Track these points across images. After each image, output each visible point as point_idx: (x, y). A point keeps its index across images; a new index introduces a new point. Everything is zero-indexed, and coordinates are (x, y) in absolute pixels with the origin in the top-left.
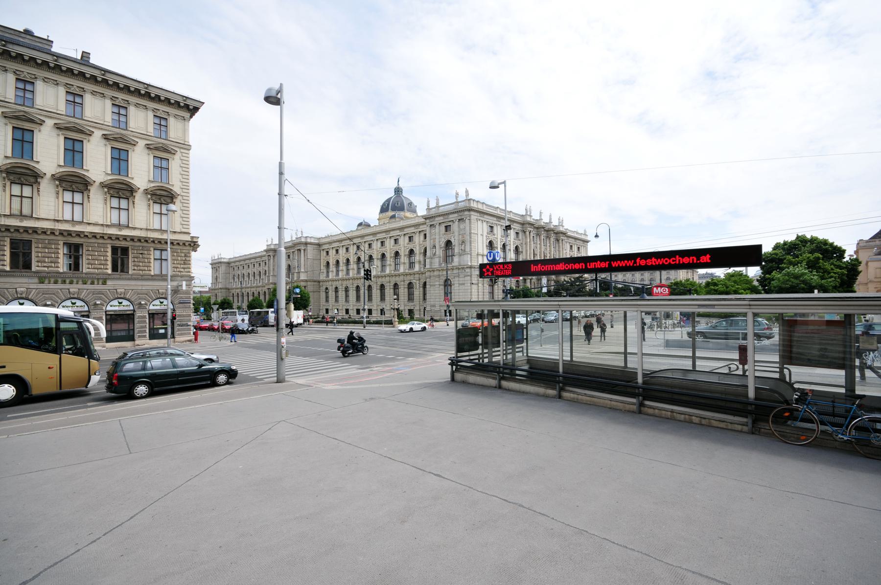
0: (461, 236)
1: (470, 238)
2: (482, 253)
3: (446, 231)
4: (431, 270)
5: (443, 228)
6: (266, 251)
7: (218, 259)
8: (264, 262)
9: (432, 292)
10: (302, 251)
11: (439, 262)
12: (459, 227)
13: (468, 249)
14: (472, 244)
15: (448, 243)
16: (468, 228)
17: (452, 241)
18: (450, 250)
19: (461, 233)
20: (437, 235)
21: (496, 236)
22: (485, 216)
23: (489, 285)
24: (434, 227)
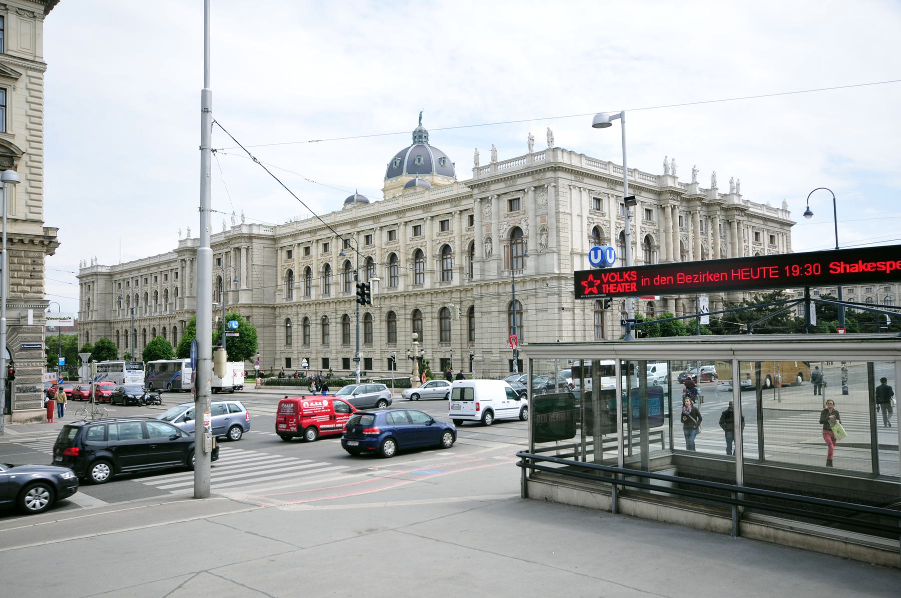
0: (539, 219)
1: (558, 221)
2: (580, 251)
3: (511, 210)
4: (483, 283)
5: (504, 204)
6: (178, 252)
7: (92, 267)
8: (174, 272)
9: (484, 325)
10: (243, 252)
11: (499, 267)
12: (535, 201)
13: (552, 243)
14: (562, 234)
15: (516, 232)
16: (552, 204)
17: (523, 227)
19: (540, 212)
20: (493, 216)
22: (586, 180)
23: (595, 312)
24: (488, 202)
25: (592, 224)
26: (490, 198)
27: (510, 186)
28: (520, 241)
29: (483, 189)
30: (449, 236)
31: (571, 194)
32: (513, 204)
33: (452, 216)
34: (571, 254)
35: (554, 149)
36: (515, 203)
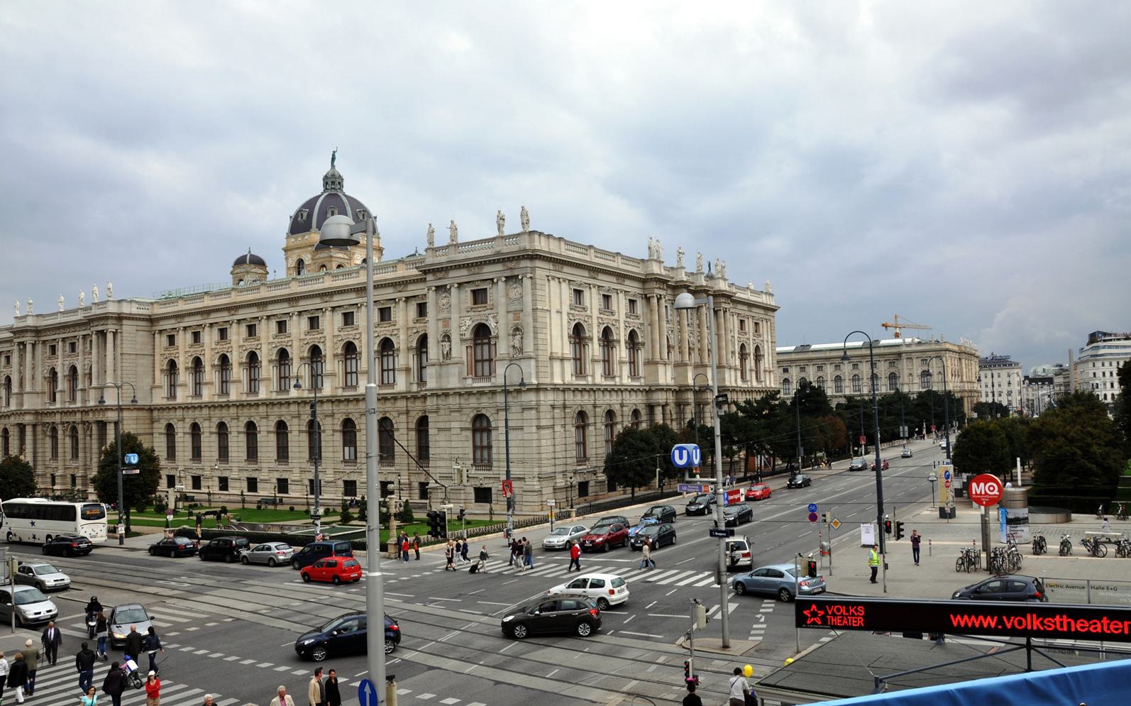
1: (535, 320)
2: (560, 355)
3: (475, 303)
5: (467, 296)
11: (460, 373)
13: (529, 348)
14: (540, 336)
15: (481, 332)
16: (528, 299)
17: (491, 324)
18: (486, 347)
19: (512, 308)
20: (453, 310)
21: (588, 313)
22: (566, 269)
23: (577, 427)
24: (445, 291)
26: (448, 287)
27: (475, 274)
28: (487, 341)
29: (439, 275)
30: (391, 328)
31: (549, 286)
32: (479, 296)
33: (396, 303)
34: (550, 359)
35: (530, 232)
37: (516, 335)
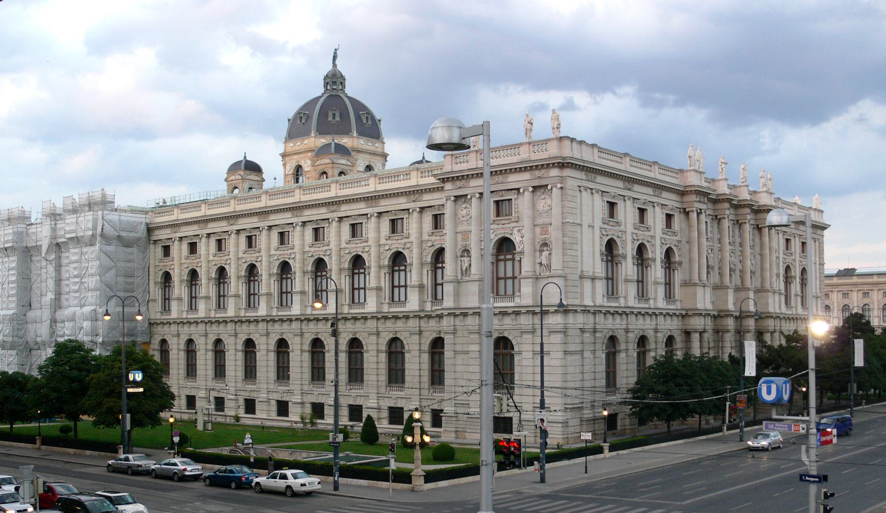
0: (538, 230)
2: (591, 274)
3: (498, 215)
4: (458, 312)
9: (459, 368)
11: (481, 292)
12: (534, 206)
15: (505, 245)
17: (516, 238)
18: (509, 264)
19: (540, 221)
20: (473, 221)
21: (622, 228)
22: (600, 179)
25: (604, 237)
26: (469, 197)
29: (458, 184)
31: (581, 198)
33: (409, 213)
34: (580, 278)
35: (561, 138)
36: (504, 207)
37: (543, 251)
